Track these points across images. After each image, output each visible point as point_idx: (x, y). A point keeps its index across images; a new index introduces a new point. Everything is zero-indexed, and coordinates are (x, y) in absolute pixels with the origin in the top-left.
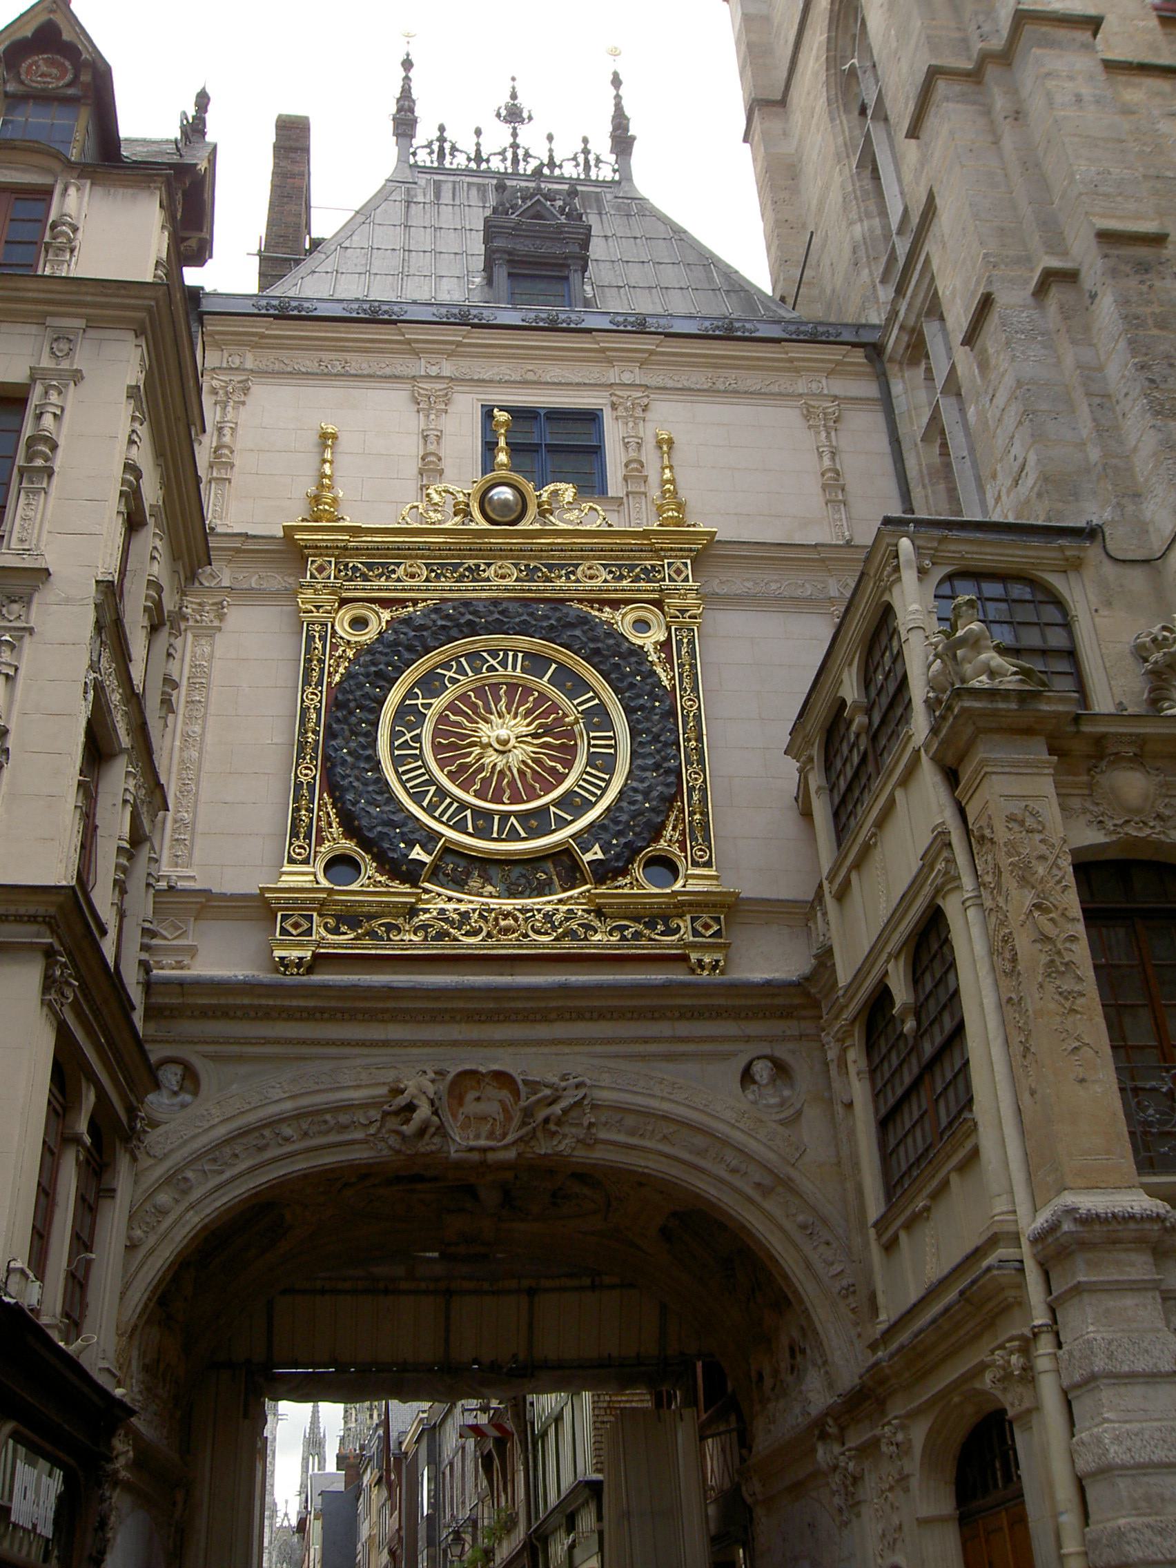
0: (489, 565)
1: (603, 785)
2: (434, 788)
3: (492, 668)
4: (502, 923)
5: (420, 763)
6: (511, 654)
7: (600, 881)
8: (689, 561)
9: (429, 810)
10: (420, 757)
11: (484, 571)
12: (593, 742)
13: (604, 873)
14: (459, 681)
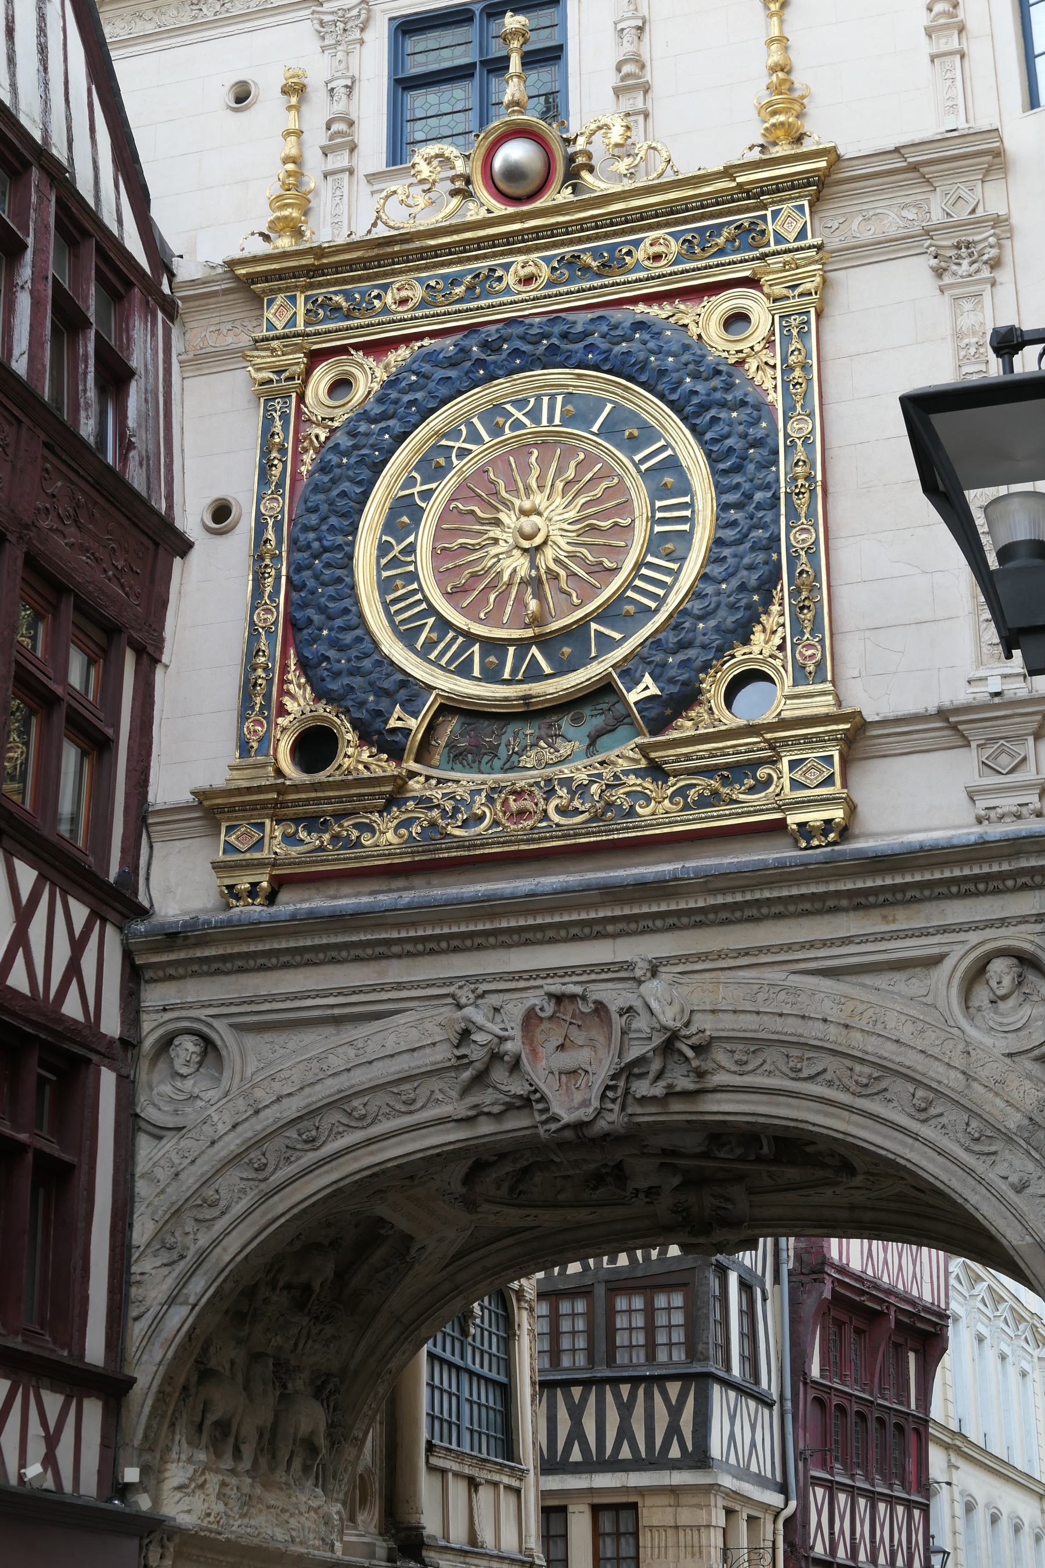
0: (507, 267)
1: (668, 579)
2: (431, 621)
3: (517, 425)
4: (514, 806)
5: (415, 586)
6: (546, 400)
7: (658, 725)
8: (806, 203)
9: (423, 654)
10: (413, 577)
11: (500, 279)
12: (659, 515)
13: (662, 714)
14: (470, 451)
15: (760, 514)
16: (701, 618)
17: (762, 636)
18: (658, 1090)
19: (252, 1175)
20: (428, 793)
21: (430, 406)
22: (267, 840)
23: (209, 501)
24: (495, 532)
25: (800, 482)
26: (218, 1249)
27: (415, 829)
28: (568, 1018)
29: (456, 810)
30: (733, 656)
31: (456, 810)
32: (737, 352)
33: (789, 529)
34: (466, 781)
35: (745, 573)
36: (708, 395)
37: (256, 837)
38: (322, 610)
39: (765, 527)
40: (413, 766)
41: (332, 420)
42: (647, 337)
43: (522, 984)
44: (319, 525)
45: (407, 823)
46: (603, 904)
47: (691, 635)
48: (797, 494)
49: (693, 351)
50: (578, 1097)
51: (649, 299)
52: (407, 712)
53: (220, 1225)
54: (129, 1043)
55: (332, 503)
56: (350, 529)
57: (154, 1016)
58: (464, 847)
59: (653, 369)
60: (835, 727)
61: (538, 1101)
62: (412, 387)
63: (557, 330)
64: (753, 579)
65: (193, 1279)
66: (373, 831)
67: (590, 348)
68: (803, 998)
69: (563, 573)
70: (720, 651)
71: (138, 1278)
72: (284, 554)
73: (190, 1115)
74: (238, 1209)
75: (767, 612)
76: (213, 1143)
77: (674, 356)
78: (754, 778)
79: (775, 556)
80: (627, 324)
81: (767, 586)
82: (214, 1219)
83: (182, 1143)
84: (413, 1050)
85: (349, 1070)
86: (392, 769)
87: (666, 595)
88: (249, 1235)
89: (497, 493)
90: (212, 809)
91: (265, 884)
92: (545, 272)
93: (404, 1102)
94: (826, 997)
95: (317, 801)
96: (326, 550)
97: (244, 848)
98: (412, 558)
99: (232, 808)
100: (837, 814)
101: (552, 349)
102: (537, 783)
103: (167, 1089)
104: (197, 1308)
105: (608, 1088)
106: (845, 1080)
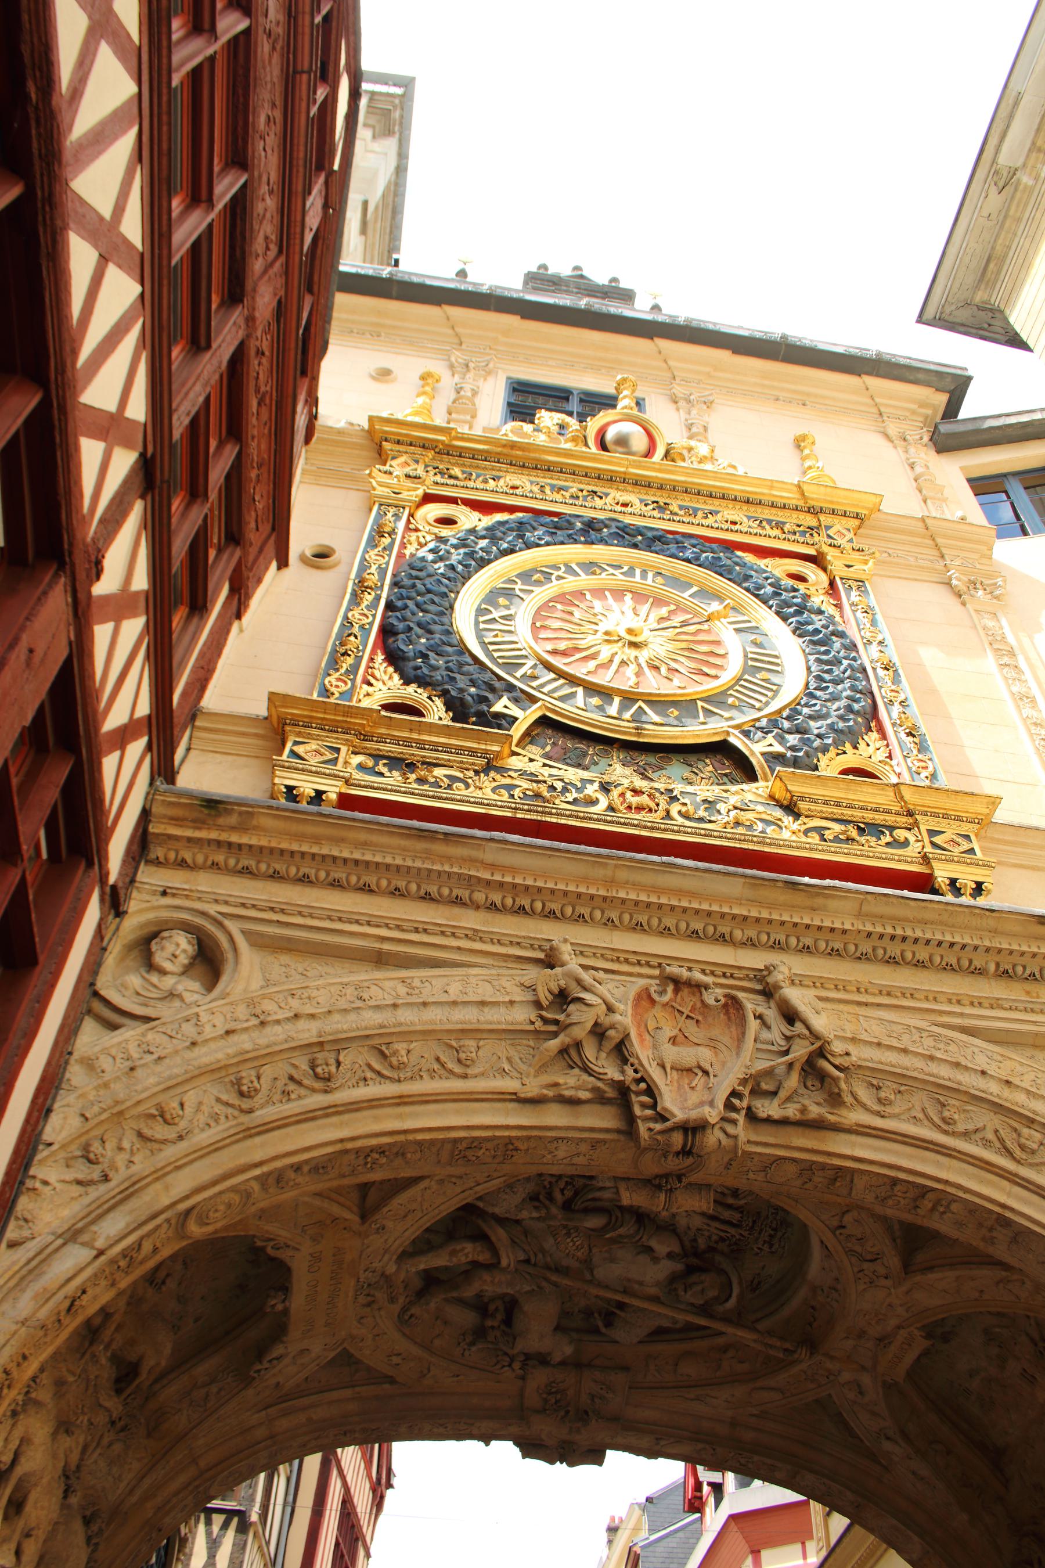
0: (607, 495)
2: (530, 663)
4: (635, 800)
12: (750, 655)
18: (791, 1111)
19: (232, 1098)
22: (341, 760)
26: (158, 1186)
27: (517, 792)
28: (686, 1012)
29: (565, 790)
31: (565, 790)
33: (880, 688)
34: (573, 774)
37: (329, 756)
43: (625, 968)
45: (510, 788)
46: (739, 901)
50: (694, 1098)
53: (170, 1153)
54: (115, 903)
57: (148, 898)
58: (577, 817)
59: (739, 573)
61: (638, 1094)
63: (650, 534)
65: (111, 1215)
68: (952, 1048)
71: (38, 1185)
73: (165, 1011)
74: (203, 1138)
76: (194, 1044)
82: (164, 1142)
83: (150, 1036)
84: (483, 1003)
85: (395, 1006)
88: (206, 1177)
90: (279, 726)
91: (333, 797)
93: (459, 1061)
94: (980, 1054)
95: (407, 742)
96: (429, 591)
102: (657, 790)
103: (135, 981)
104: (103, 1258)
105: (734, 1094)
106: (1009, 1144)
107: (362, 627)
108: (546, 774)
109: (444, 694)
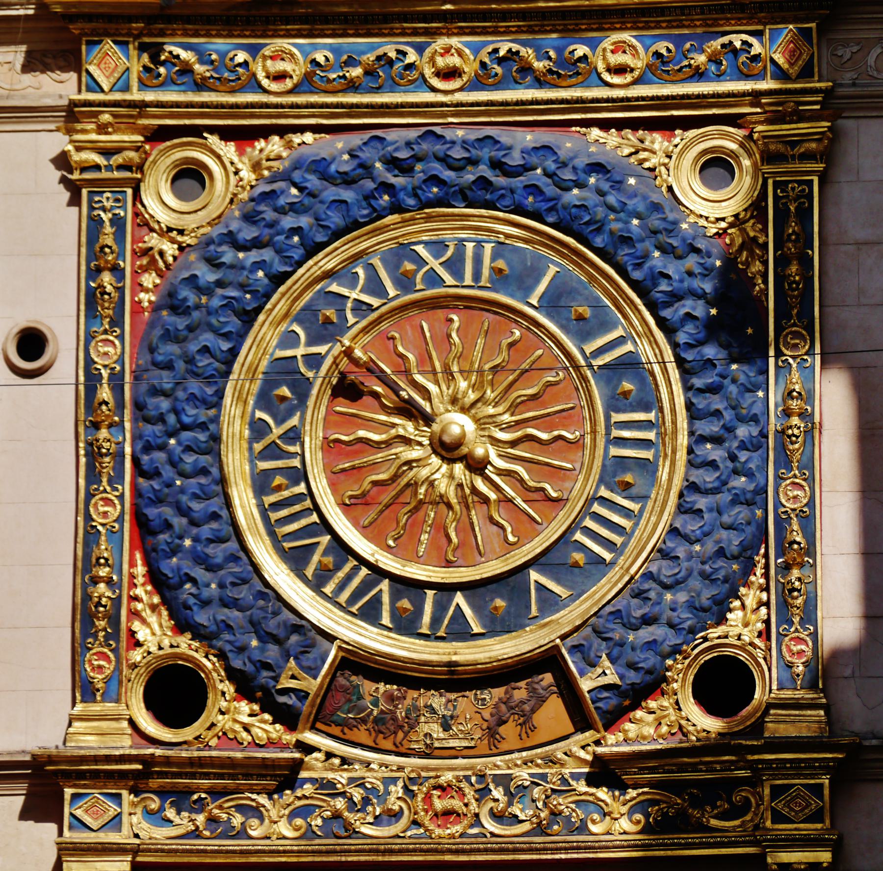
3: (433, 279)
5: (302, 488)
6: (470, 246)
7: (613, 719)
9: (317, 584)
10: (300, 475)
12: (616, 433)
14: (370, 308)
15: (743, 456)
16: (667, 587)
17: (739, 614)
20: (330, 775)
21: (320, 238)
22: (125, 818)
23: (16, 330)
24: (407, 428)
25: (795, 420)
30: (705, 639)
31: (366, 801)
32: (718, 220)
33: (779, 478)
34: (376, 766)
35: (724, 534)
36: (681, 281)
38: (184, 511)
39: (750, 475)
40: (310, 737)
41: (181, 232)
42: (605, 186)
44: (173, 390)
45: (304, 812)
47: (657, 609)
48: (789, 437)
49: (663, 209)
51: (605, 125)
52: (302, 668)
55: (190, 361)
56: (215, 399)
59: (611, 233)
60: (830, 756)
62: (294, 208)
63: (486, 153)
64: (733, 541)
66: (261, 818)
67: (533, 189)
69: (493, 496)
70: (692, 631)
72: (127, 425)
75: (747, 585)
77: (639, 216)
78: (730, 801)
79: (759, 512)
80: (581, 162)
81: (749, 552)
86: (277, 731)
87: (625, 545)
89: (406, 373)
92: (470, 69)
96: (185, 427)
97: (94, 825)
98: (296, 449)
99: (81, 775)
100: (825, 857)
101: (483, 182)
102: (467, 778)
107: (111, 532)
108: (344, 782)
109: (222, 656)
